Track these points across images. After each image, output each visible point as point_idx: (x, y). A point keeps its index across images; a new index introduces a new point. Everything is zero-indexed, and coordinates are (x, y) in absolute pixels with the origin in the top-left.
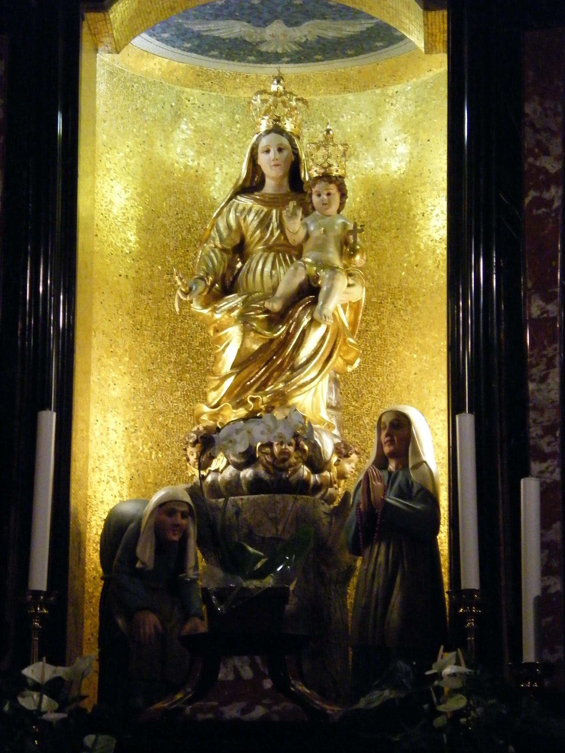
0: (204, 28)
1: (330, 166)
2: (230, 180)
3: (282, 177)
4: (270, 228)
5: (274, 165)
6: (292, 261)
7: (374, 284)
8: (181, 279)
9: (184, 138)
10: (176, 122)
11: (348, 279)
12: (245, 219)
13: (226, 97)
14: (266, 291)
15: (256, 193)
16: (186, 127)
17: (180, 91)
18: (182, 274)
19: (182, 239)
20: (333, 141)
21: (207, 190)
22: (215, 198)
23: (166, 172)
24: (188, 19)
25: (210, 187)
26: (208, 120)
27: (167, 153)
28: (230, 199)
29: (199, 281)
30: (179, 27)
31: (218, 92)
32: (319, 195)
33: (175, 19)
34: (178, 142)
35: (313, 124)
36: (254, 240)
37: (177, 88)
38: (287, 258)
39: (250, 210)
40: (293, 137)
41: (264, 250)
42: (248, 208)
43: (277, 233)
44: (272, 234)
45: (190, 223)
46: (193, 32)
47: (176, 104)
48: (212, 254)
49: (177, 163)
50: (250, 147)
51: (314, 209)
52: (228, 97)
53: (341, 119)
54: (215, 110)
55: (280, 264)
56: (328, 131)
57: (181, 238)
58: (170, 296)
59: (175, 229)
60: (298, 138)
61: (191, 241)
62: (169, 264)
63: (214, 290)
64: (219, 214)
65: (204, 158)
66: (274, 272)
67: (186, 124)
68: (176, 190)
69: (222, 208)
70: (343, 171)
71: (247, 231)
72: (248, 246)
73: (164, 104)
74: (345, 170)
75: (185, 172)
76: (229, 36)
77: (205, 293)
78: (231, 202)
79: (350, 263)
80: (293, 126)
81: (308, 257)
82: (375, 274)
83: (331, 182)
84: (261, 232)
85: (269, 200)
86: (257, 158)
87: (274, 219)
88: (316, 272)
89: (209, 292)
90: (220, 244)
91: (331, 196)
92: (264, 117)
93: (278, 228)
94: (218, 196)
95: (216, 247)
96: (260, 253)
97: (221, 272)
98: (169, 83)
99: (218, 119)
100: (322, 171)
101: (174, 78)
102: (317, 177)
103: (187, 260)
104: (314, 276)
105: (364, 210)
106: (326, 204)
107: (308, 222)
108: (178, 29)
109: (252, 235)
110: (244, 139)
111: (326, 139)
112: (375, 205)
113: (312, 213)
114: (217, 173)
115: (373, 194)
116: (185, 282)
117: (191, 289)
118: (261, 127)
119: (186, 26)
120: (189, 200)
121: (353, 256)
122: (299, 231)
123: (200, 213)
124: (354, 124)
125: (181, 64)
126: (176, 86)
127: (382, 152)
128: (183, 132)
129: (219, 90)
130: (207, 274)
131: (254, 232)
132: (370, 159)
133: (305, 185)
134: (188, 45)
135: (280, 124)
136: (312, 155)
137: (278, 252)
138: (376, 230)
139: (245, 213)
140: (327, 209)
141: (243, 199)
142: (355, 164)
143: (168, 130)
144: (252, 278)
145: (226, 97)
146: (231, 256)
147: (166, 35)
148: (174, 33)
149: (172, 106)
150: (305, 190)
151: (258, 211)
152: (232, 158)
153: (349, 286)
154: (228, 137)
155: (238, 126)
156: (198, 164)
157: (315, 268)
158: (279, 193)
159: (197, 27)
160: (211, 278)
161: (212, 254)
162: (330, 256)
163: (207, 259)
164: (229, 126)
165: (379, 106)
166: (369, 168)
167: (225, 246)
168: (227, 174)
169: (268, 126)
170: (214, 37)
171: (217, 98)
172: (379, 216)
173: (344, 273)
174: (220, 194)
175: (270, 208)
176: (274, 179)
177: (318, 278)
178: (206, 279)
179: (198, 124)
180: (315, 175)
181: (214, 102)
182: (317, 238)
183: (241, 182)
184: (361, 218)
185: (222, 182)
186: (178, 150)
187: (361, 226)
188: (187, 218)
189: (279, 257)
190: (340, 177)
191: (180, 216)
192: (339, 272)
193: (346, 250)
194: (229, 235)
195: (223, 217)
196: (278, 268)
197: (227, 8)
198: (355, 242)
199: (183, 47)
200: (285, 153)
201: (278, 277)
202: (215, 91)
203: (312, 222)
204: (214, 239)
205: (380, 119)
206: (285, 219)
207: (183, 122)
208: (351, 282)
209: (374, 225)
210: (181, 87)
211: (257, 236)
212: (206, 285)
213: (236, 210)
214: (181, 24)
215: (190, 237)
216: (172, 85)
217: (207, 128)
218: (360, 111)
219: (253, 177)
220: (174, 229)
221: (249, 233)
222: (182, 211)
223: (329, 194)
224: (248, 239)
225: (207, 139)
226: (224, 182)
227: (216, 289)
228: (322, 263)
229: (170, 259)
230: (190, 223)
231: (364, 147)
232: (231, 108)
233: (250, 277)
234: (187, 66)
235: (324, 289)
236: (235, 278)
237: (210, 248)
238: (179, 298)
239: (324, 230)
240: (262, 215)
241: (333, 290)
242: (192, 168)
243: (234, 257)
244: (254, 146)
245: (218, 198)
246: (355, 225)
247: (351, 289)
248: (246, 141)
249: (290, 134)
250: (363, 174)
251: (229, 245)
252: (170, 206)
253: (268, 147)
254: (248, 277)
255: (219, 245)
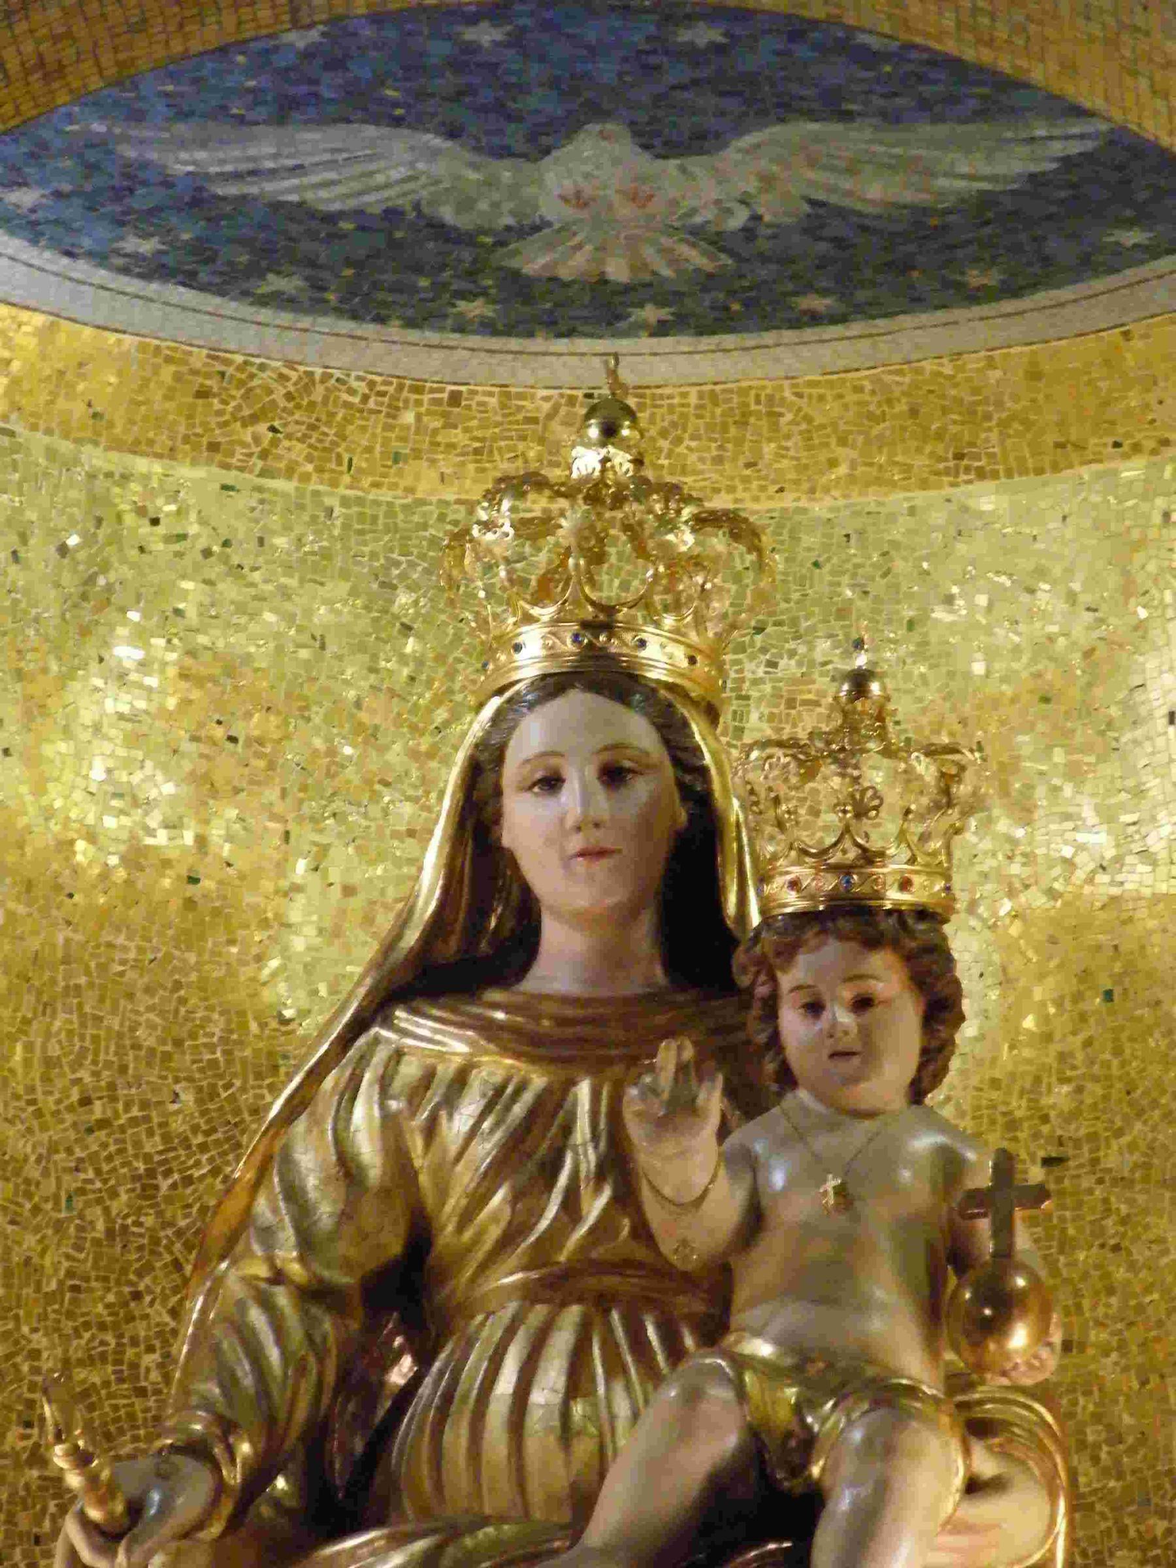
0: (223, 162)
1: (869, 857)
2: (368, 920)
3: (627, 915)
4: (563, 1179)
5: (582, 854)
6: (676, 1353)
7: (1120, 1476)
8: (82, 1459)
9: (125, 709)
10: (85, 631)
11: (967, 1452)
12: (431, 1130)
13: (345, 502)
14: (537, 1515)
15: (495, 995)
16: (139, 654)
17: (109, 475)
18: (88, 1428)
19: (110, 1233)
20: (883, 736)
21: (247, 972)
22: (288, 1013)
23: (29, 885)
24: (137, 116)
25: (260, 959)
26: (254, 615)
27: (39, 789)
28: (359, 1026)
29: (186, 1464)
30: (92, 156)
31: (305, 478)
32: (814, 1008)
33: (70, 118)
34: (97, 728)
35: (797, 637)
36: (477, 1240)
37: (96, 458)
38: (651, 1332)
39: (460, 1080)
40: (685, 711)
41: (530, 1294)
42: (446, 1071)
43: (595, 1206)
44: (571, 1206)
45: (154, 1145)
46: (167, 183)
47: (89, 540)
48: (257, 1317)
49: (92, 837)
50: (460, 758)
51: (787, 1078)
52: (360, 501)
53: (940, 614)
54: (288, 569)
55: (614, 1368)
56: (859, 681)
57: (100, 1225)
58: (37, 1540)
59: (71, 1182)
60: (712, 713)
61: (155, 1241)
62: (36, 1371)
63: (266, 1511)
64: (296, 1106)
65: (233, 813)
66: (578, 1409)
67: (140, 636)
68: (82, 980)
69: (317, 1074)
70: (939, 885)
71: (443, 1193)
72: (443, 1275)
73: (24, 538)
74: (948, 878)
75: (129, 883)
76: (352, 204)
77: (215, 1529)
78: (362, 1041)
79: (980, 1367)
80: (680, 655)
81: (758, 1333)
82: (1127, 1419)
83: (872, 943)
84: (516, 1197)
85: (558, 1032)
86: (497, 818)
87: (582, 1129)
88: (798, 1410)
89: (235, 1522)
90: (302, 1259)
91: (877, 1011)
92: (535, 611)
93: (600, 1177)
94: (304, 1003)
95: (279, 1277)
96: (512, 1307)
97: (301, 1413)
98: (49, 432)
99: (309, 613)
100: (829, 883)
101: (79, 409)
102: (803, 918)
103: (134, 1342)
104: (789, 1435)
105: (1063, 1080)
106: (848, 1054)
107: (759, 1148)
108: (92, 168)
109: (466, 1217)
110: (441, 715)
111: (850, 724)
112: (1118, 1052)
113: (780, 1095)
114: (297, 888)
115: (1108, 996)
116: (105, 1474)
117: (135, 1510)
118: (520, 658)
119: (130, 152)
120: (152, 1026)
121: (996, 1327)
122: (706, 1191)
123: (206, 1096)
124: (1005, 636)
125: (112, 338)
126: (88, 449)
127: (1152, 782)
128: (122, 677)
129: (310, 468)
130: (227, 1427)
131: (479, 1199)
132: (1088, 814)
133: (740, 957)
134: (148, 247)
135: (615, 647)
136: (777, 801)
137: (602, 1302)
138: (1128, 1183)
139: (435, 1096)
140: (855, 1079)
141: (424, 1027)
142: (1014, 842)
143: (45, 670)
144: (464, 1441)
145: (345, 502)
146: (354, 1326)
147: (25, 198)
148: (66, 187)
149: (63, 550)
150: (744, 981)
151: (499, 1091)
152: (375, 811)
153: (974, 1487)
154: (358, 704)
155: (411, 646)
156: (201, 841)
157: (791, 1393)
158: (603, 992)
159: (184, 155)
160: (245, 1448)
161: (257, 1317)
162: (876, 1325)
163: (230, 1346)
164: (362, 648)
165: (1140, 545)
166: (1086, 865)
167: (326, 1274)
168: (349, 891)
169: (553, 656)
170: (277, 206)
171: (301, 507)
172: (1140, 1113)
173: (945, 1420)
174: (315, 992)
175: (562, 1073)
176: (580, 920)
177: (808, 1443)
178: (218, 1450)
179: (202, 639)
180: (793, 902)
181: (287, 528)
182: (807, 1231)
183: (412, 937)
184: (1045, 1119)
185: (321, 931)
186: (98, 773)
187: (1048, 1162)
188: (134, 1122)
189: (609, 1329)
190: (922, 913)
191: (98, 1110)
192: (919, 1415)
193: (956, 1294)
194: (346, 1216)
195: (317, 1122)
196: (601, 1390)
197: (336, 64)
198: (1005, 1253)
199: (118, 253)
200: (641, 790)
201: (601, 1435)
202: (289, 473)
203: (782, 1144)
204: (267, 1235)
205: (1143, 613)
206: (636, 1130)
207: (121, 631)
208: (986, 1466)
209: (1113, 1158)
210: (114, 456)
211: (494, 1218)
212: (220, 1487)
213: (384, 1084)
214: (101, 144)
215: (149, 1221)
216: (65, 447)
217: (248, 658)
218: (1041, 573)
219: (480, 911)
220: (67, 1178)
221: (455, 1202)
222: (112, 1086)
223: (863, 1004)
224: (447, 1235)
225: (248, 715)
226: (333, 933)
227: (276, 1503)
228: (830, 1366)
229: (39, 1340)
230: (154, 1145)
231: (1059, 756)
232: (374, 556)
233: (457, 1437)
234: (142, 348)
235: (842, 1502)
236: (383, 1435)
237: (250, 1281)
238: (73, 1554)
239: (840, 1191)
240: (519, 1110)
241: (889, 1514)
242: (167, 863)
243: (373, 1326)
244: (484, 757)
245: (304, 1014)
246: (1005, 1165)
247: (984, 1510)
248: (447, 724)
249: (663, 693)
250: (1052, 894)
251: (347, 1265)
252: (49, 1063)
253: (554, 761)
254: (448, 1436)
255: (295, 1270)
